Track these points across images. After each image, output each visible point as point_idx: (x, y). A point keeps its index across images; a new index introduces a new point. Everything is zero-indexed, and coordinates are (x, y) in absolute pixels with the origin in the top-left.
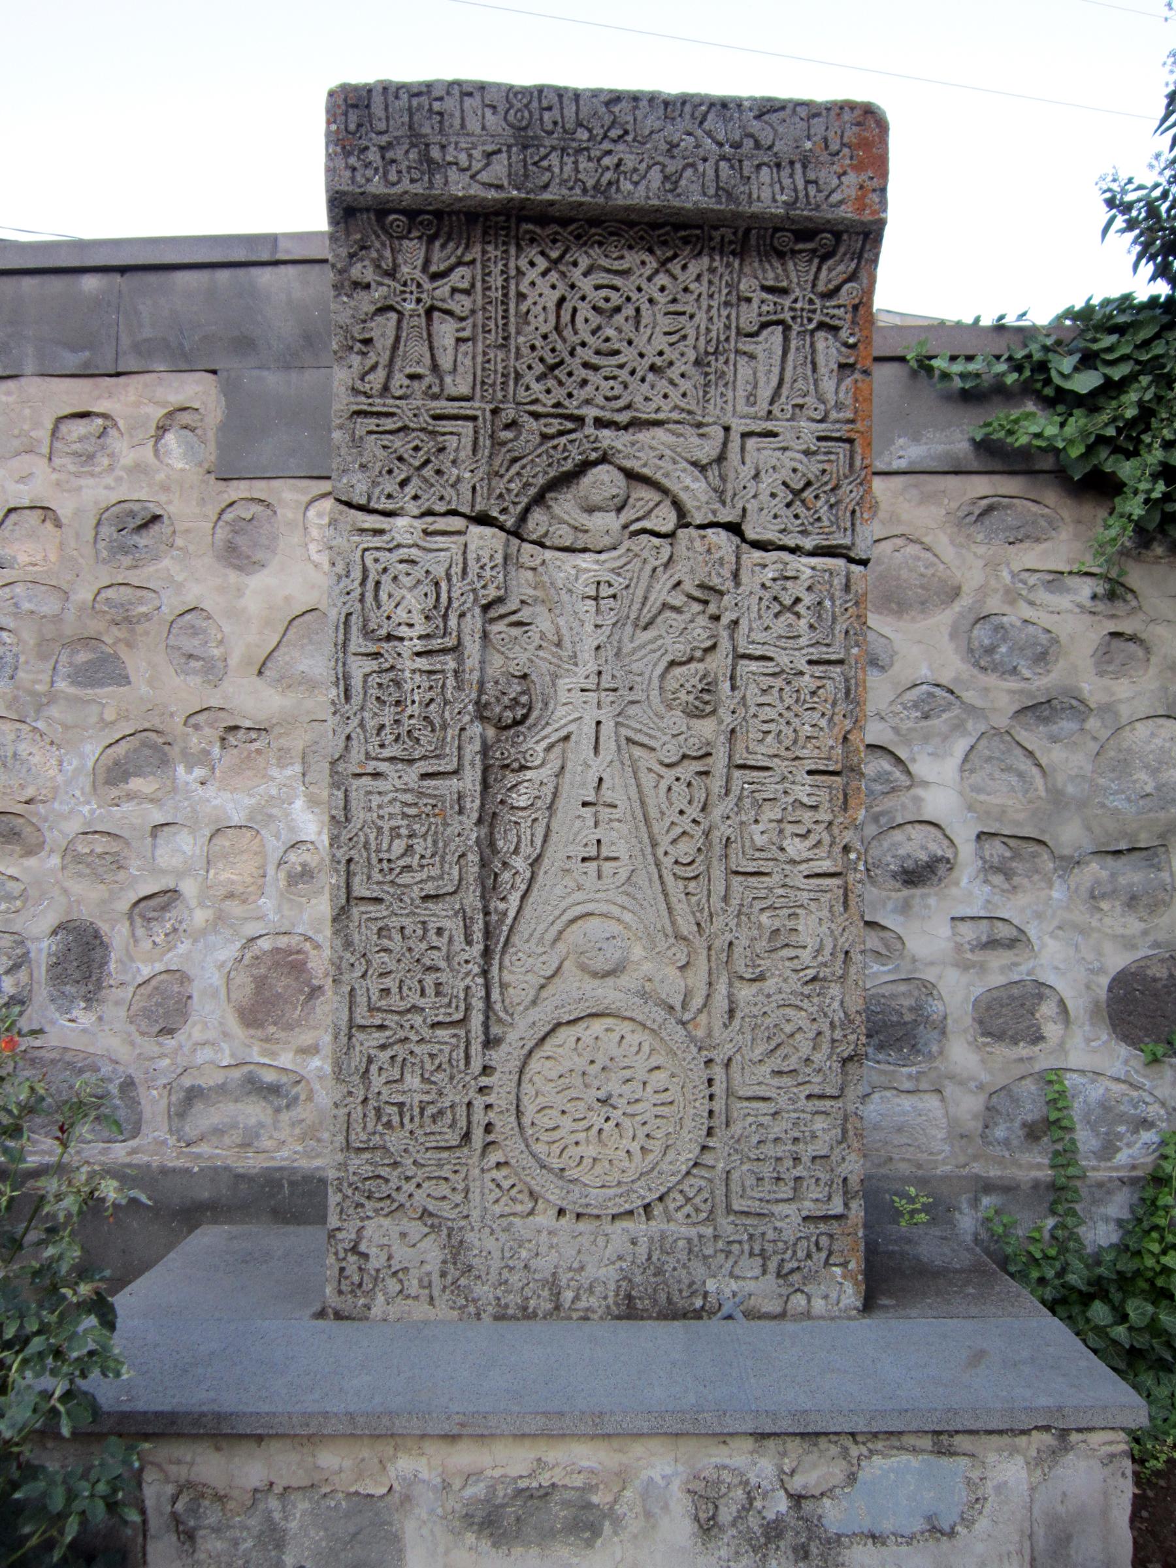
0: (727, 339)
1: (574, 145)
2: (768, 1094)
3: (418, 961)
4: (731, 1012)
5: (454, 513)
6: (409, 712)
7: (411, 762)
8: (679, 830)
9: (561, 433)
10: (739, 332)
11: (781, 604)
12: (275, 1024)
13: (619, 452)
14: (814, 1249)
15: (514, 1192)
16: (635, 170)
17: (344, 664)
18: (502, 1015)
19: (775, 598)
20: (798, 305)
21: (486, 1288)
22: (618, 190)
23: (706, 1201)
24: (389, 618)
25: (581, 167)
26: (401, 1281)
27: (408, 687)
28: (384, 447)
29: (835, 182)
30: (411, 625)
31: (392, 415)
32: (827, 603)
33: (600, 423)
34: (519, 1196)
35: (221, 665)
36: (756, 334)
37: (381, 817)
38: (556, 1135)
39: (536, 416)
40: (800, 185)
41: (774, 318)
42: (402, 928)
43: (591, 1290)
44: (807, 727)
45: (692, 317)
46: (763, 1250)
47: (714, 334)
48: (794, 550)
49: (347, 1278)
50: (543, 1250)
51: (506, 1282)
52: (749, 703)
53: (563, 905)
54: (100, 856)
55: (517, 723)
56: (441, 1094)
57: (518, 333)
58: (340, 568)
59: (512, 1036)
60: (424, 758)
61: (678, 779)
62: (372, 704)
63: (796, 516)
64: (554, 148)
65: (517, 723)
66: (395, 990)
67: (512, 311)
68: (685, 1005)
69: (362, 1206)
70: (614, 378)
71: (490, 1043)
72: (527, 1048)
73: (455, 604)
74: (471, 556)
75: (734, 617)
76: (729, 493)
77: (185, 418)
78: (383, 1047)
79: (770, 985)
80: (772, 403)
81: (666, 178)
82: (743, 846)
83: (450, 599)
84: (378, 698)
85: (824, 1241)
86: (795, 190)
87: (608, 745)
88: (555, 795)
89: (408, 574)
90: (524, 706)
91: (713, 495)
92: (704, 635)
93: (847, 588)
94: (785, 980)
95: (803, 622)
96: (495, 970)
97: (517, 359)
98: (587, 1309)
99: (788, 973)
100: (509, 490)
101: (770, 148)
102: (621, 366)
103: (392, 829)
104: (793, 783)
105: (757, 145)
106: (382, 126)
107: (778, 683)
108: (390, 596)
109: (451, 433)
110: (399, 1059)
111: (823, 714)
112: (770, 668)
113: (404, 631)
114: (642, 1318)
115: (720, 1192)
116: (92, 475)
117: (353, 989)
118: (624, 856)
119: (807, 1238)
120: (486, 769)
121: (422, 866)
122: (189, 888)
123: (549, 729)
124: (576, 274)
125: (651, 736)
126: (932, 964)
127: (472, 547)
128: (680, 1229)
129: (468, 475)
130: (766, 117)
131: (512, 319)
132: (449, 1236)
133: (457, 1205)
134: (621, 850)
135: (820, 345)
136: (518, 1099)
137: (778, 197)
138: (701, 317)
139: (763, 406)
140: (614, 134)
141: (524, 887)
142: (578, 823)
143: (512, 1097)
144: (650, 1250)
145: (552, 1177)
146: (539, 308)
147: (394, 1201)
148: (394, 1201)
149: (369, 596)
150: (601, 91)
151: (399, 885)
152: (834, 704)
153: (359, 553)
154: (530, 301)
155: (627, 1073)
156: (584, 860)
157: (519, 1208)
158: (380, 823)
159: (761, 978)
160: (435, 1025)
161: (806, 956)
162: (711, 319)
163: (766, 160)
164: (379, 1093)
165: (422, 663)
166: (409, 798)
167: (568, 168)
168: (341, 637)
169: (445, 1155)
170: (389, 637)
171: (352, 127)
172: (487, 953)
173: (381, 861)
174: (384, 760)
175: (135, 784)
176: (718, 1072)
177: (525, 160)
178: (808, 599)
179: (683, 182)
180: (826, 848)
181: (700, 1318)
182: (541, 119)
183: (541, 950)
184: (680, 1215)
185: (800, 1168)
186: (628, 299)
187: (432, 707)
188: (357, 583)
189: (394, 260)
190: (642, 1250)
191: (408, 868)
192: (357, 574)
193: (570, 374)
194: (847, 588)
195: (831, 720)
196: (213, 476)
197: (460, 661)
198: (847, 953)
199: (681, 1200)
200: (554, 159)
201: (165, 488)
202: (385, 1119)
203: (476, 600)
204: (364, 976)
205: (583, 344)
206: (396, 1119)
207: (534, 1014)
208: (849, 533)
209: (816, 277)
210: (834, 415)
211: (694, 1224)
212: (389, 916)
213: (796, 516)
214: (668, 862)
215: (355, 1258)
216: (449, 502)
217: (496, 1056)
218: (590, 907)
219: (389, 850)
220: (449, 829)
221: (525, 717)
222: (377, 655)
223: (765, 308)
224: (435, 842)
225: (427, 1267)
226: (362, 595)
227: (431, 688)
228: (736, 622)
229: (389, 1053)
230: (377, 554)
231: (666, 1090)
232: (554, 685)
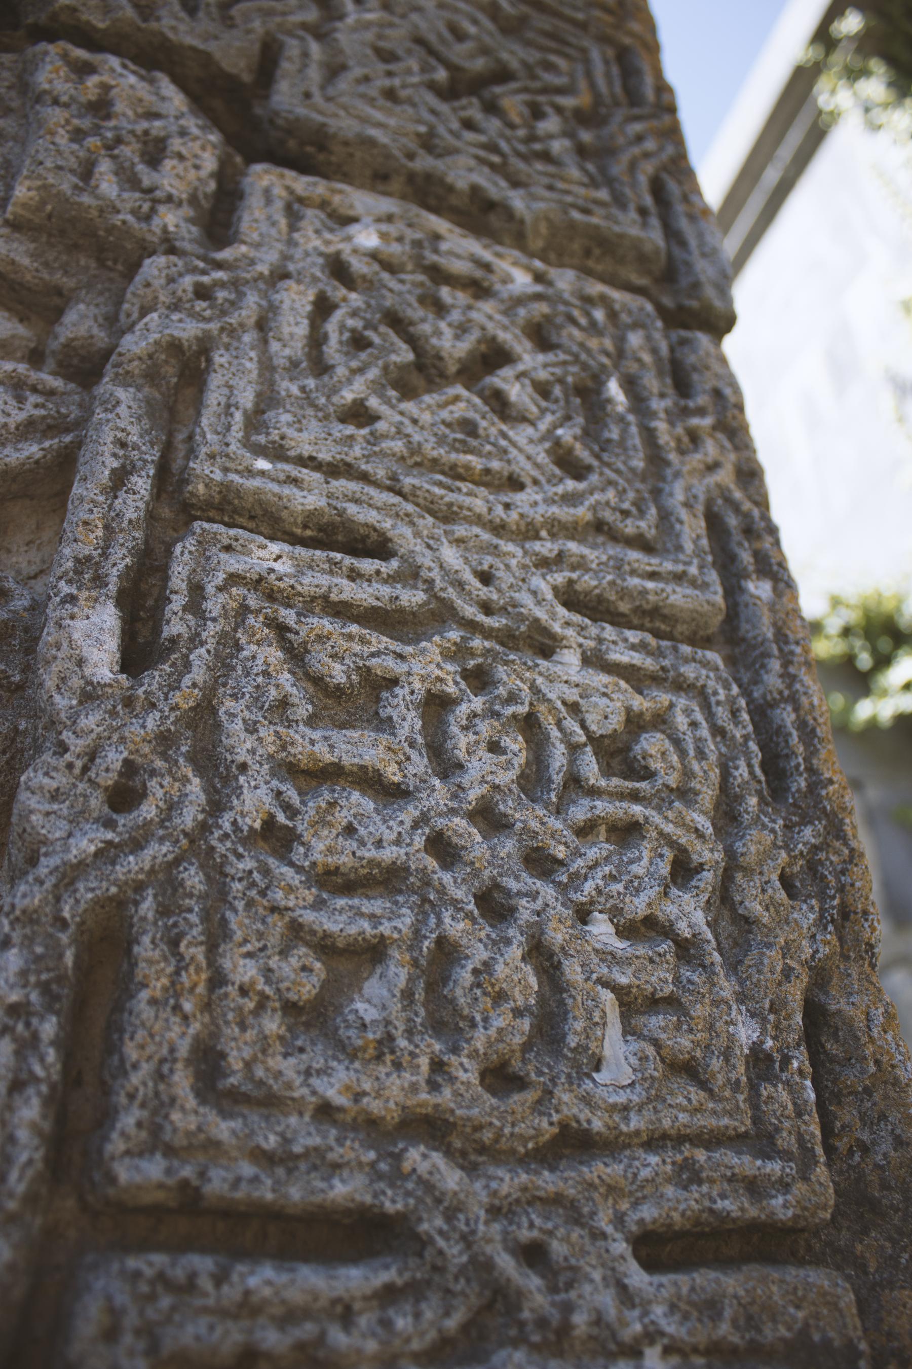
52: (240, 744)
107: (426, 664)
111: (683, 870)
152: (727, 815)
195: (724, 899)
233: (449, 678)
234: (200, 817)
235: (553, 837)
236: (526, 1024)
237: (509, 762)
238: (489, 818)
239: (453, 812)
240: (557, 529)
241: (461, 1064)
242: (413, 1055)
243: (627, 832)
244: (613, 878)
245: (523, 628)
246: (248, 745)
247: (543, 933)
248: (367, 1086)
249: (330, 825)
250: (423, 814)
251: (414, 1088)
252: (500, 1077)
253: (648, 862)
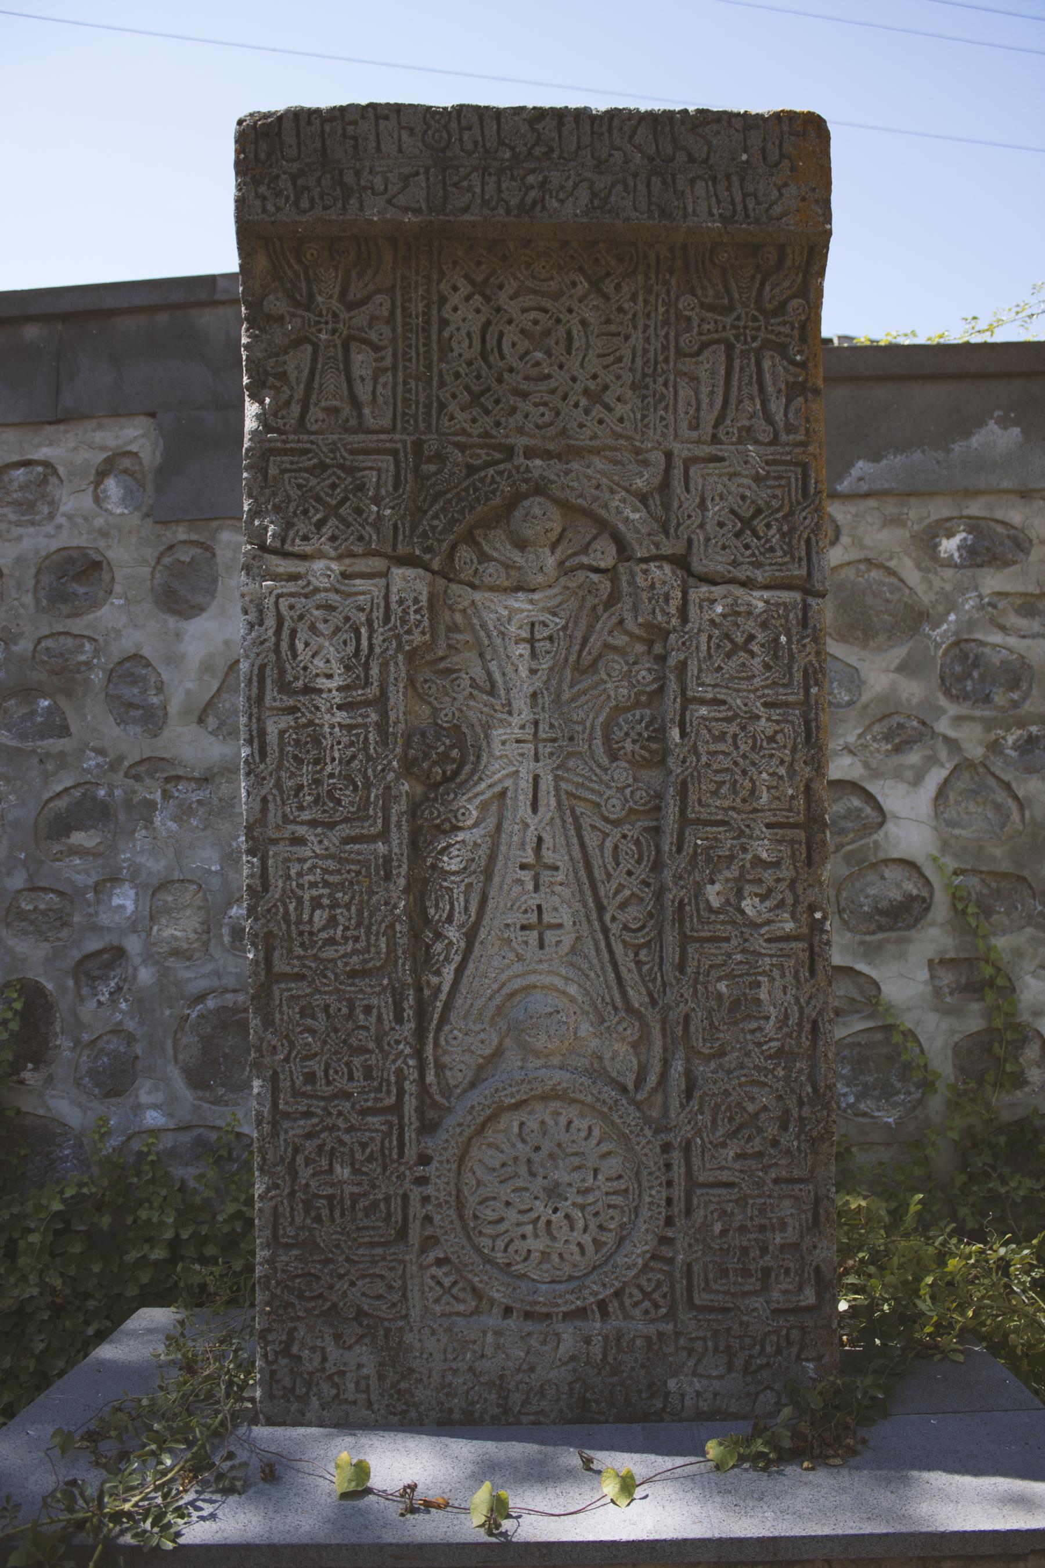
0: (666, 360)
1: (496, 164)
2: (732, 1179)
3: (345, 1042)
4: (689, 1093)
5: (375, 554)
6: (329, 769)
7: (331, 826)
8: (627, 893)
9: (488, 465)
10: (680, 354)
11: (732, 641)
12: (223, 1085)
13: (552, 482)
14: (783, 1343)
15: (455, 1291)
16: (562, 187)
17: (259, 719)
18: (438, 1098)
19: (727, 636)
20: (741, 323)
21: (428, 1393)
22: (544, 208)
23: (664, 1296)
24: (305, 668)
25: (504, 186)
26: (336, 1385)
27: (327, 742)
28: (300, 487)
29: (775, 193)
30: (329, 676)
31: (308, 451)
32: (783, 639)
33: (530, 453)
34: (461, 1295)
35: (161, 713)
36: (698, 353)
37: (301, 886)
38: (502, 1227)
39: (462, 447)
40: (738, 199)
41: (716, 336)
42: (327, 1007)
43: (541, 1392)
44: (764, 775)
45: (627, 338)
46: (728, 1347)
47: (651, 355)
48: (747, 584)
49: (278, 1381)
50: (489, 1351)
51: (450, 1385)
52: (701, 750)
53: (504, 977)
54: (44, 913)
55: (447, 779)
56: (374, 1187)
57: (441, 360)
58: (252, 617)
59: (450, 1121)
60: (346, 820)
61: (624, 837)
62: (289, 763)
63: (747, 547)
64: (475, 169)
65: (447, 779)
66: (320, 1074)
67: (434, 338)
68: (639, 1082)
69: (293, 1305)
70: (545, 404)
71: (428, 1128)
72: (466, 1134)
73: (378, 650)
74: (394, 598)
75: (682, 657)
76: (674, 523)
77: (126, 463)
78: (309, 1136)
79: (730, 1059)
80: (716, 426)
81: (594, 195)
82: (698, 910)
83: (371, 647)
84: (295, 757)
85: (795, 1334)
86: (733, 203)
87: (548, 801)
88: (492, 858)
89: (326, 621)
90: (454, 760)
91: (655, 525)
92: (650, 678)
93: (804, 622)
94: (747, 1054)
95: (758, 660)
96: (429, 1051)
97: (439, 388)
98: (538, 1413)
99: (751, 1046)
100: (433, 528)
101: (706, 161)
102: (553, 392)
103: (312, 899)
104: (751, 837)
105: (691, 159)
106: (293, 152)
107: (733, 728)
108: (307, 644)
109: (371, 468)
110: (327, 1148)
111: (782, 762)
112: (723, 712)
113: (322, 683)
114: (599, 1422)
115: (681, 1285)
116: (32, 523)
117: (275, 1073)
118: (568, 922)
119: (777, 1332)
120: (415, 833)
121: (346, 939)
122: (133, 945)
123: (483, 785)
124: (503, 298)
125: (593, 791)
126: (909, 1009)
127: (394, 589)
128: (639, 1327)
129: (388, 512)
130: (700, 130)
131: (435, 347)
132: (386, 1337)
133: (394, 1305)
134: (565, 917)
135: (766, 364)
136: (459, 1190)
137: (715, 211)
138: (637, 338)
139: (707, 429)
140: (538, 151)
141: (458, 958)
142: (517, 889)
143: (452, 1187)
144: (605, 1348)
145: (496, 1273)
146: (463, 332)
147: (326, 1300)
148: (326, 1300)
149: (284, 645)
150: (523, 108)
151: (322, 960)
152: (794, 750)
153: (273, 599)
154: (452, 328)
155: (576, 1161)
156: (523, 928)
157: (461, 1308)
158: (300, 893)
159: (722, 1053)
160: (365, 1112)
161: (770, 1027)
162: (647, 340)
163: (701, 172)
164: (307, 1185)
165: (341, 717)
166: (331, 864)
167: (491, 187)
168: (255, 691)
169: (379, 1251)
170: (308, 690)
171: (263, 156)
172: (420, 1033)
173: (301, 934)
174: (302, 823)
175: (78, 838)
176: (676, 1157)
177: (444, 182)
178: (761, 637)
179: (613, 199)
180: (789, 908)
181: (662, 1420)
182: (461, 140)
183: (478, 1027)
184: (637, 1312)
185: (768, 1258)
186: (558, 321)
187: (356, 763)
188: (270, 633)
189: (310, 289)
190: (596, 1350)
191: (331, 941)
192: (270, 622)
193: (497, 402)
194: (804, 622)
196: (150, 520)
197: (384, 715)
198: (815, 1023)
199: (638, 1296)
200: (475, 179)
201: (104, 534)
202: (313, 1214)
203: (400, 647)
204: (287, 1059)
205: (511, 370)
206: (325, 1213)
207: (474, 1098)
208: (804, 563)
209: (760, 294)
210: (783, 437)
211: (653, 1321)
212: (312, 994)
213: (747, 547)
214: (614, 928)
215: (286, 1361)
216: (369, 543)
217: (430, 1144)
218: (532, 979)
219: (311, 921)
220: (374, 899)
221: (456, 773)
222: (292, 710)
223: (706, 327)
224: (360, 912)
225: (365, 1371)
226: (277, 645)
227: (352, 744)
228: (683, 665)
229: (317, 1142)
230: (293, 600)
231: (620, 1177)
232: (487, 736)
238: (744, 756)
240: (764, 687)
243: (772, 756)
252: (744, 801)
253: (774, 762)
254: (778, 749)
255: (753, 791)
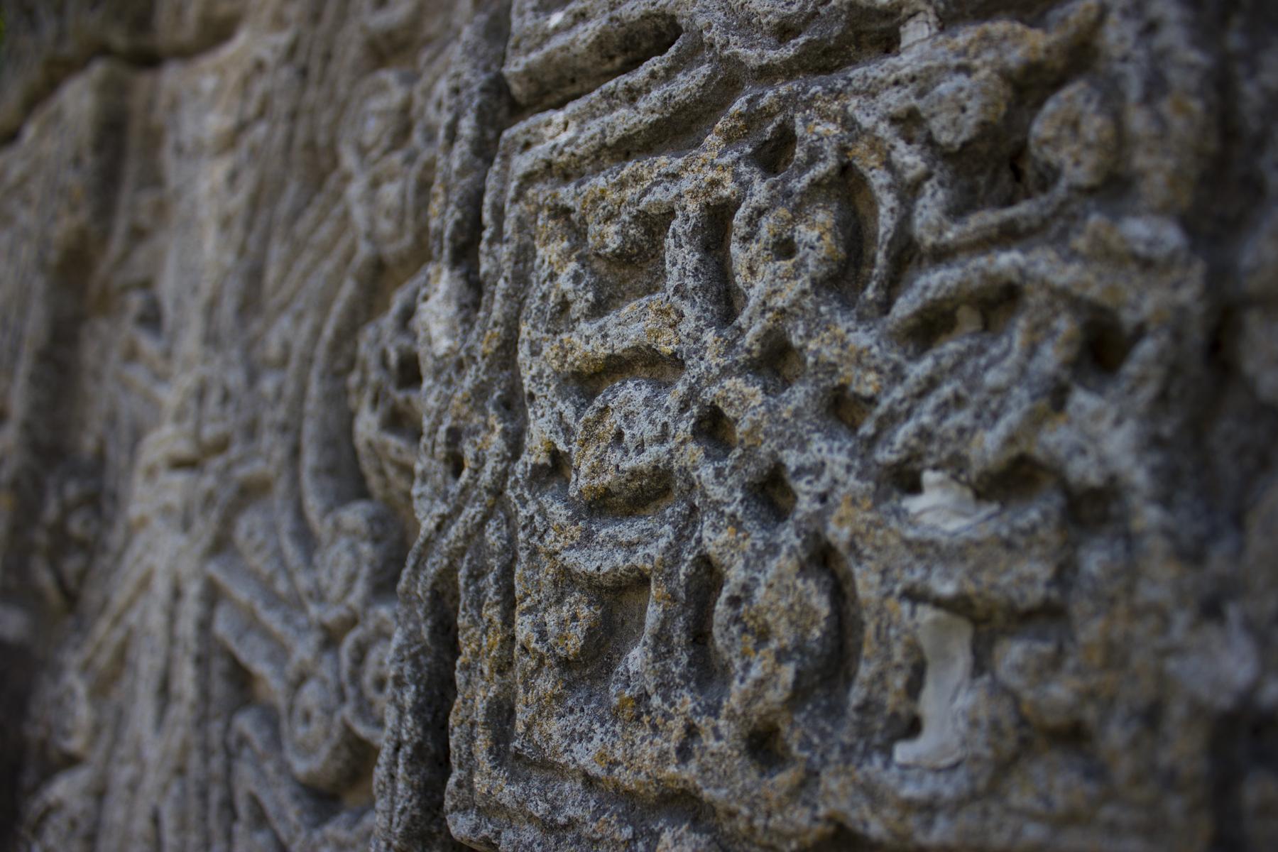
111: (1101, 349)
233: (727, 175)
234: (499, 468)
235: (858, 362)
236: (788, 673)
237: (801, 265)
238: (774, 361)
239: (725, 371)
241: (715, 729)
242: (667, 716)
244: (958, 401)
245: (837, 30)
246: (534, 371)
247: (824, 524)
248: (618, 754)
249: (599, 438)
250: (691, 388)
251: (663, 757)
252: (763, 745)
254: (1052, 231)
255: (829, 665)
